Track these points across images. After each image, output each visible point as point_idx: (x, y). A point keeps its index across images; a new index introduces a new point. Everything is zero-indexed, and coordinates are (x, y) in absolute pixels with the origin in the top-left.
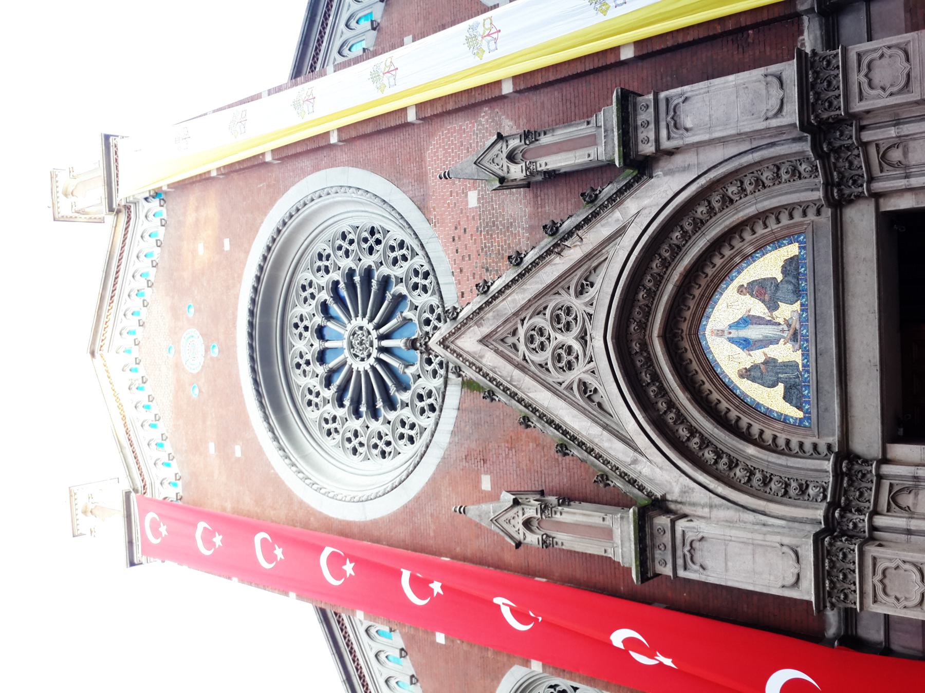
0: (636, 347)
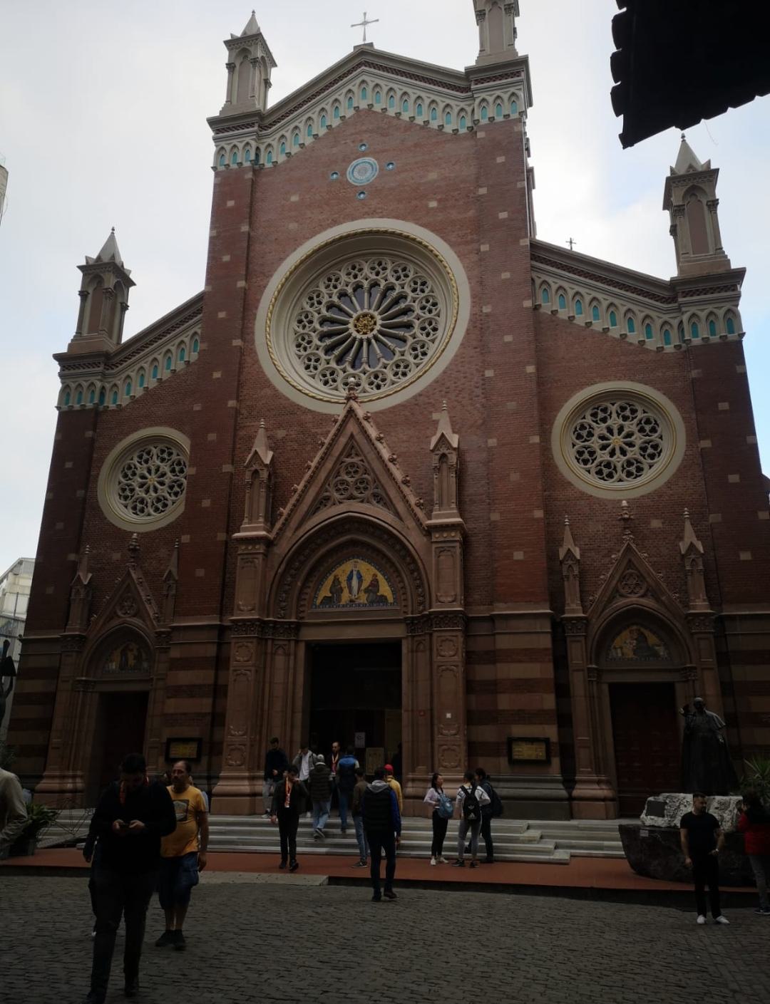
0: (347, 527)
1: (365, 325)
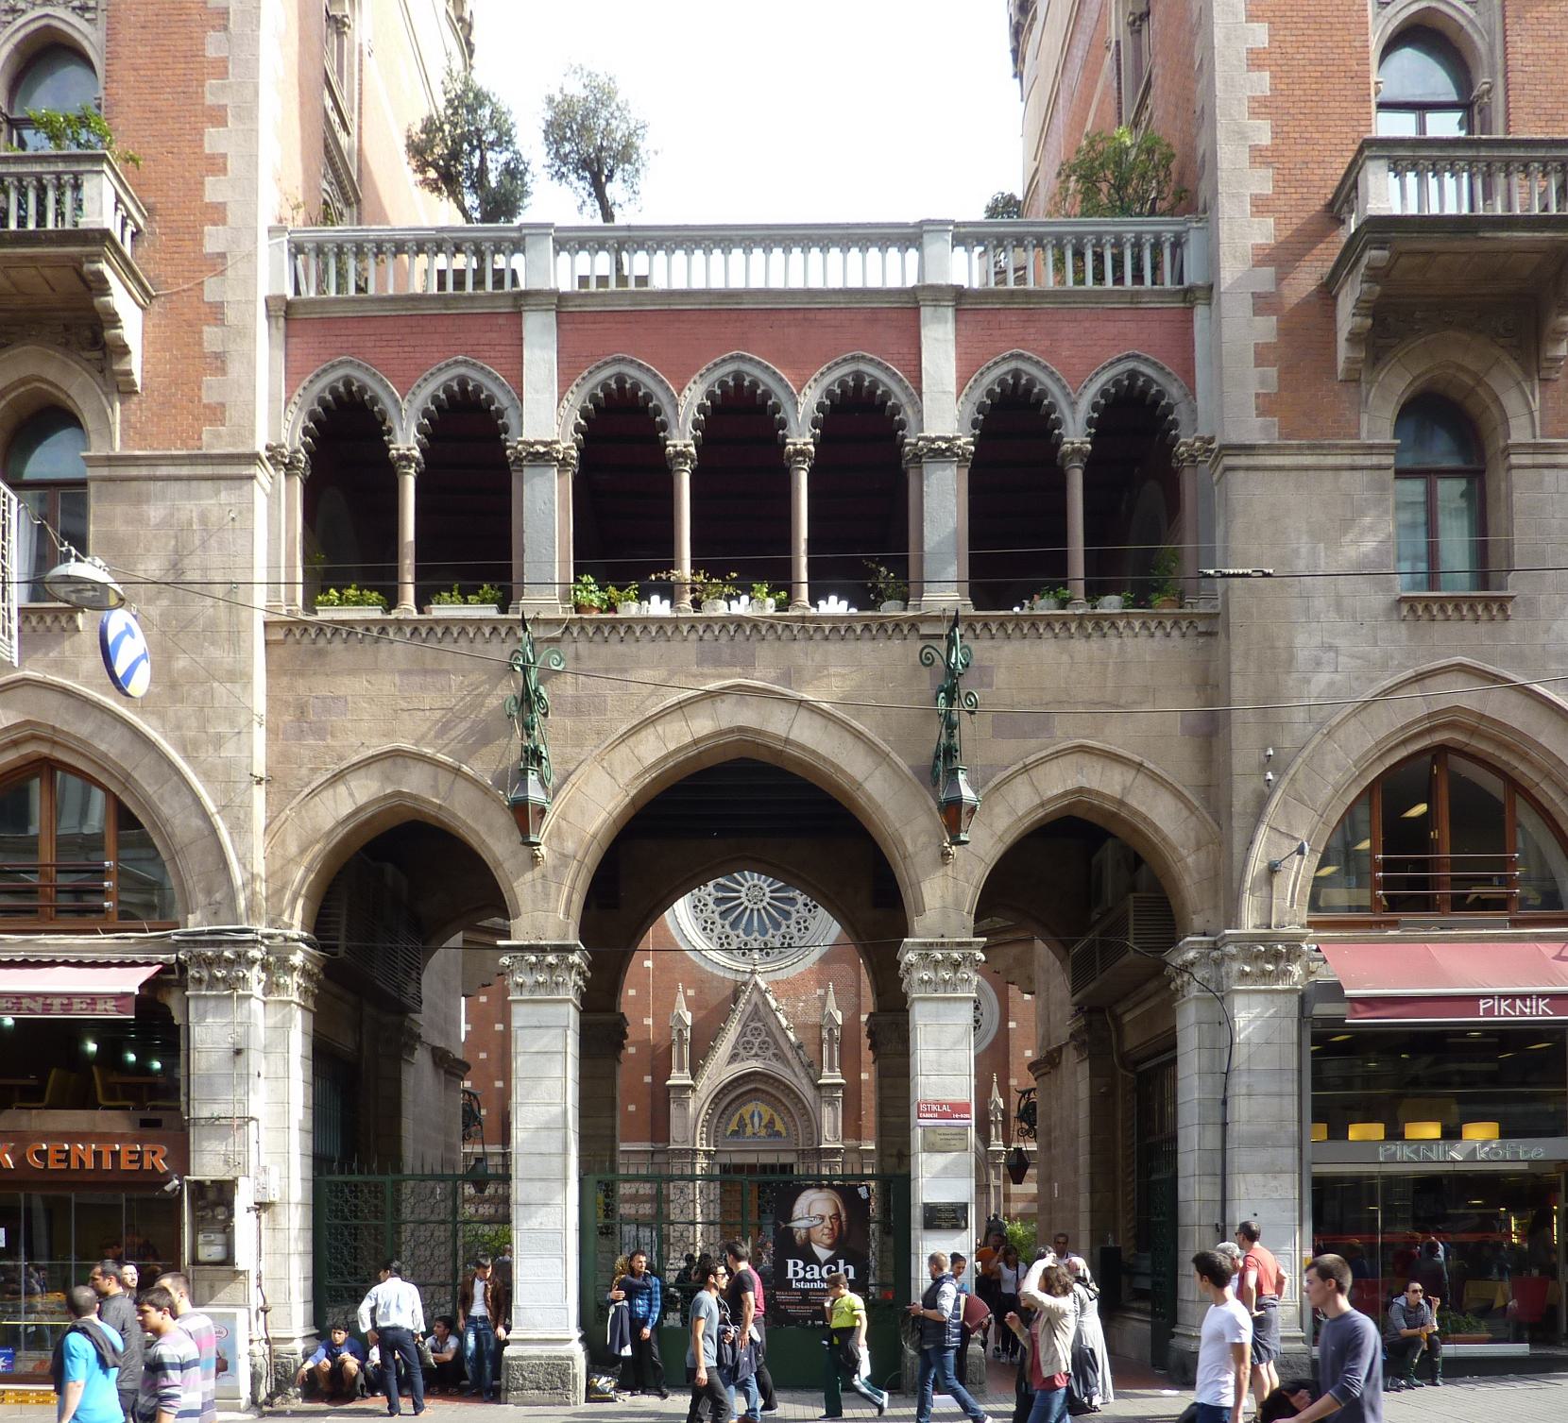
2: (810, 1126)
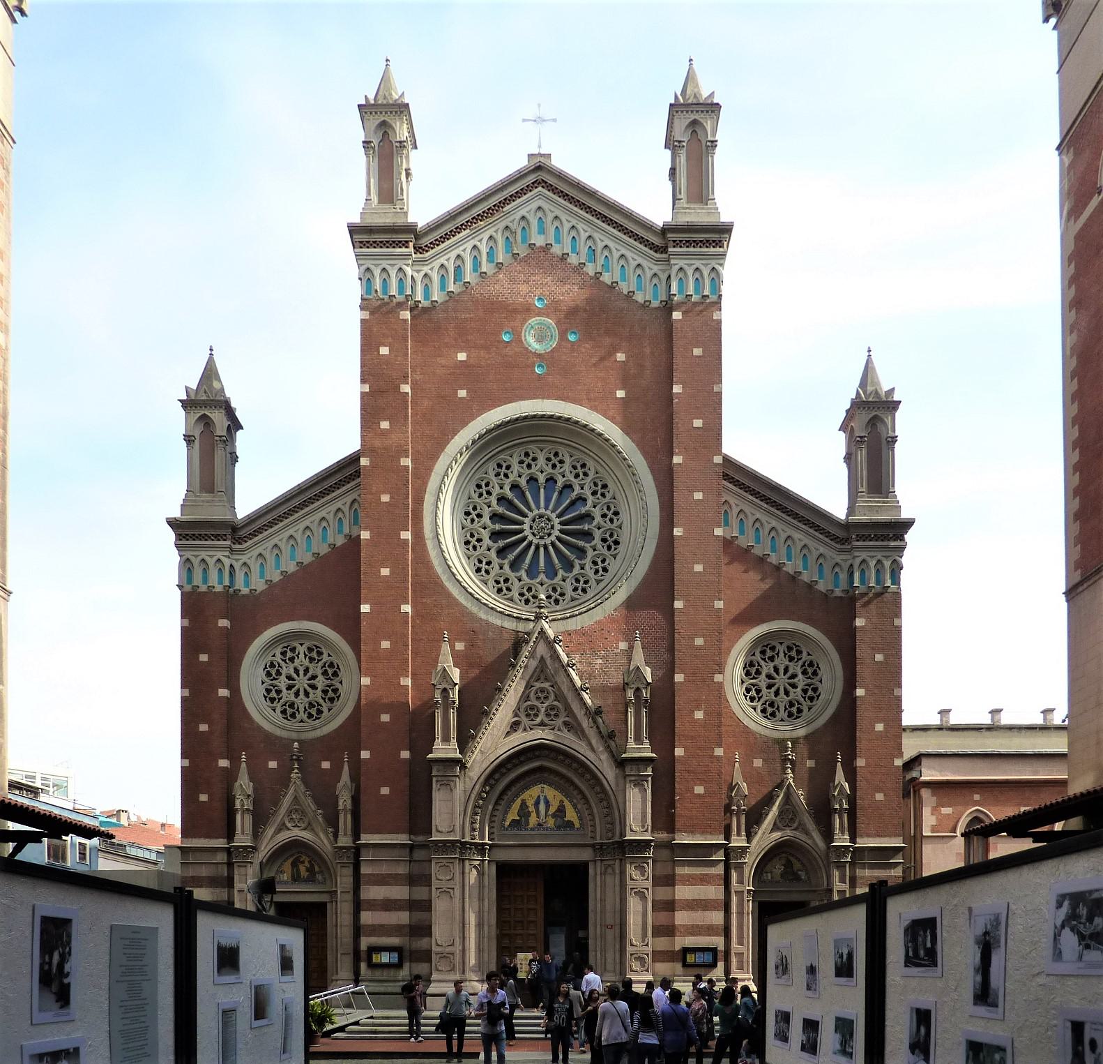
1: (542, 528)
2: (610, 814)
